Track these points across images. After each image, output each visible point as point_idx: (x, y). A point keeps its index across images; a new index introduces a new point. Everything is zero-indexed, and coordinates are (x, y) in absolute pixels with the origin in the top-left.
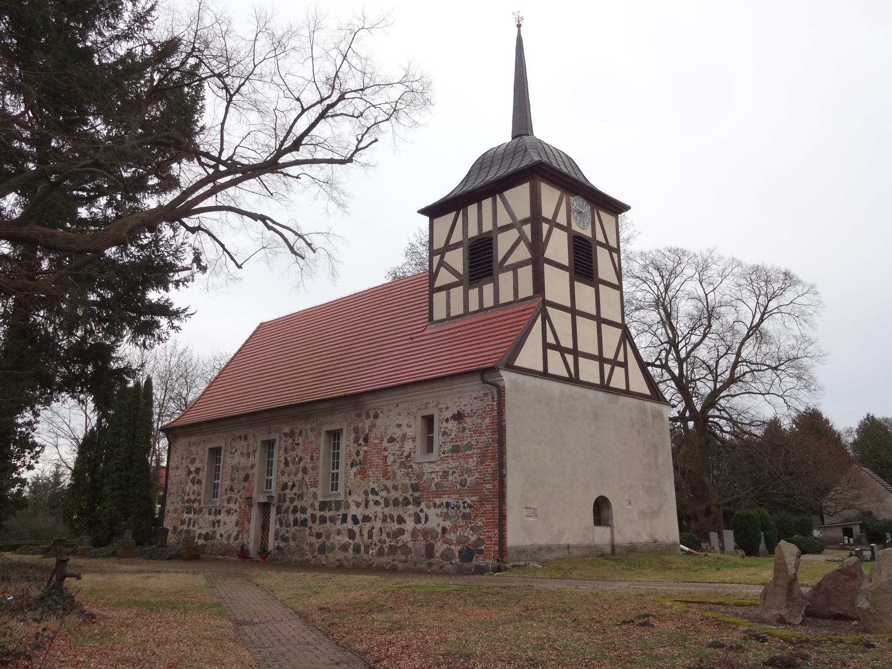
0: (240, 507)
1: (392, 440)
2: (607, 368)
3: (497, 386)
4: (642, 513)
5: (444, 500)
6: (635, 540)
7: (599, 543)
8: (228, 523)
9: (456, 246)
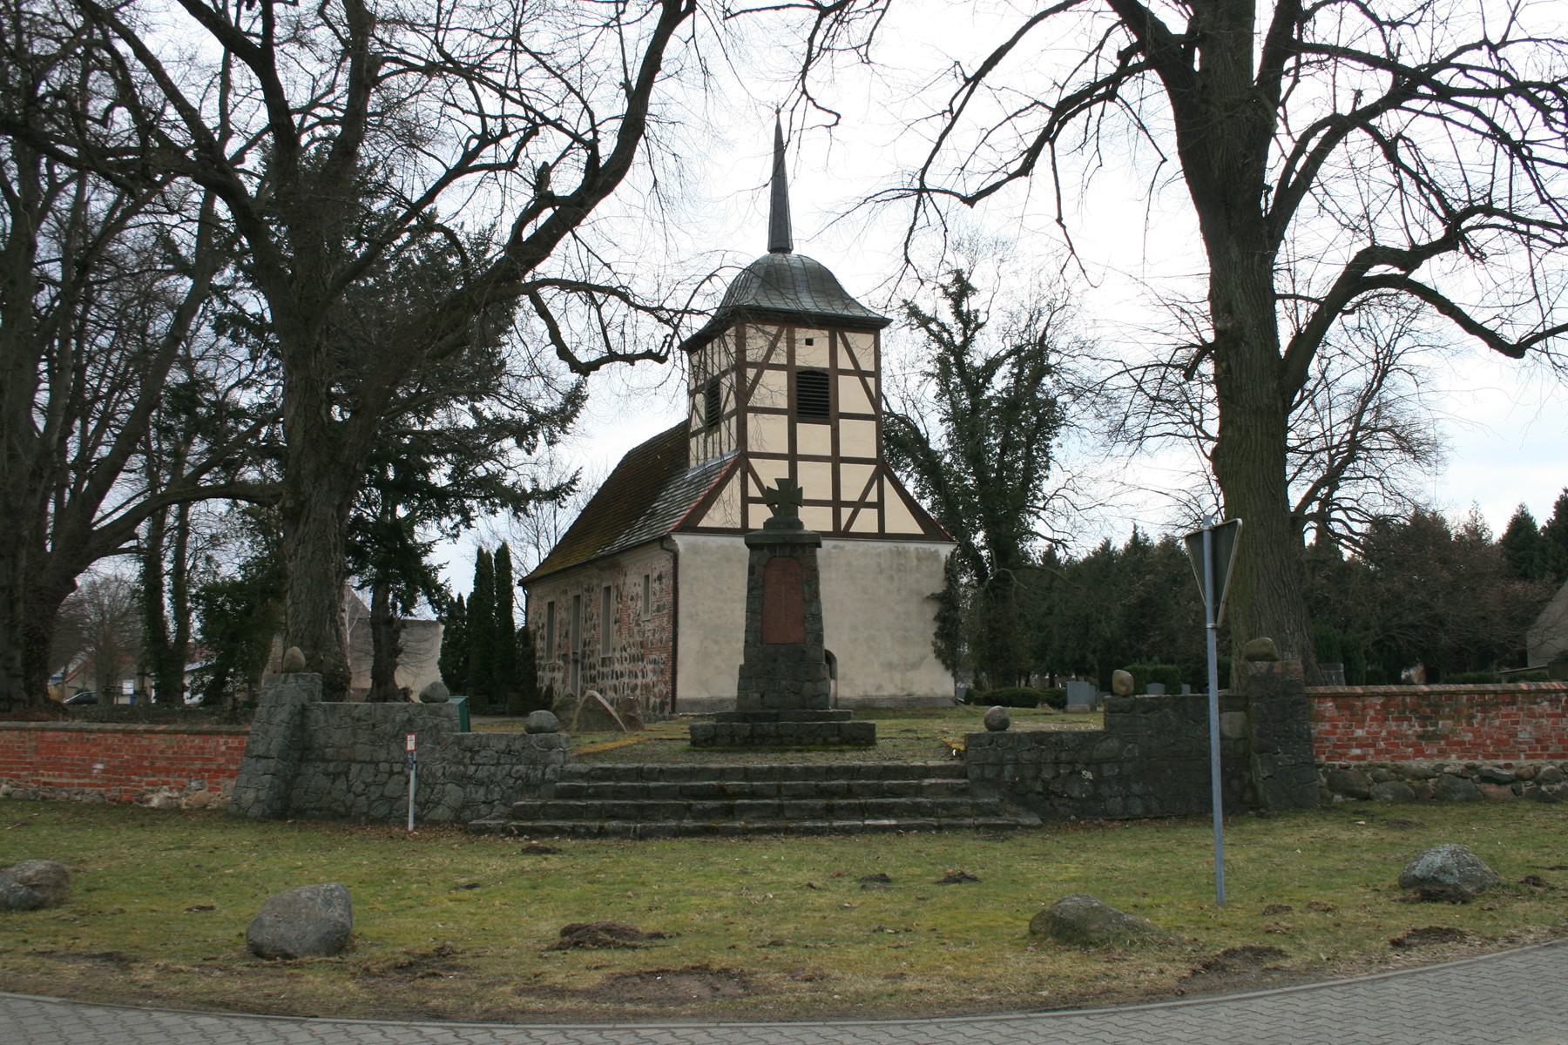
1: (632, 599)
2: (846, 513)
3: (671, 551)
4: (890, 666)
6: (873, 693)
9: (702, 385)
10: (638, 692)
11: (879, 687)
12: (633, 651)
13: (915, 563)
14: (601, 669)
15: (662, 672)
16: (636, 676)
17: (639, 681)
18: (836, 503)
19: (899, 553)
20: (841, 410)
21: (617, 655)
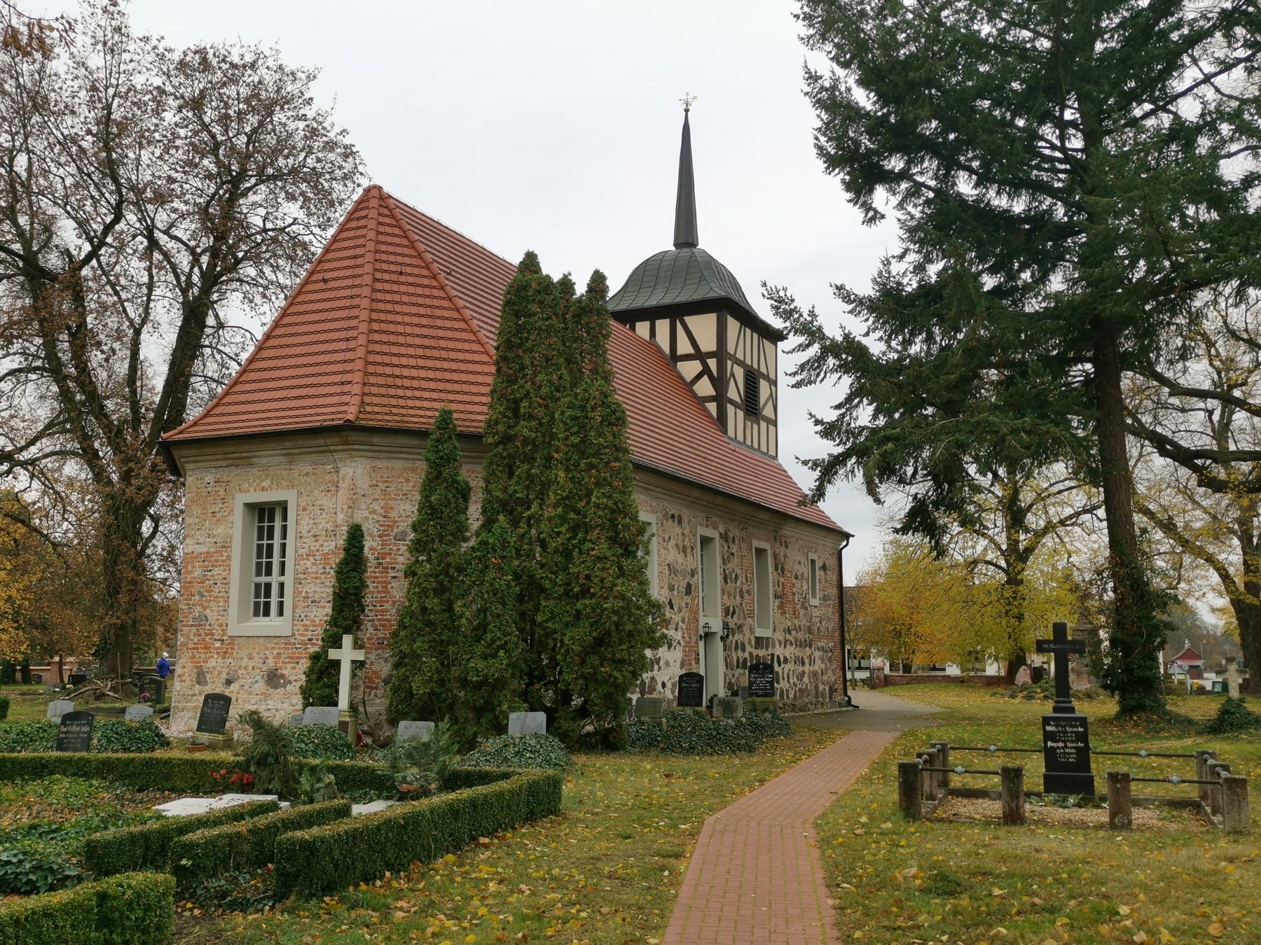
0: (683, 637)
5: (823, 644)
8: (672, 663)
10: (806, 679)
12: (801, 635)
14: (755, 652)
15: (830, 660)
16: (803, 664)
17: (807, 668)
21: (779, 636)
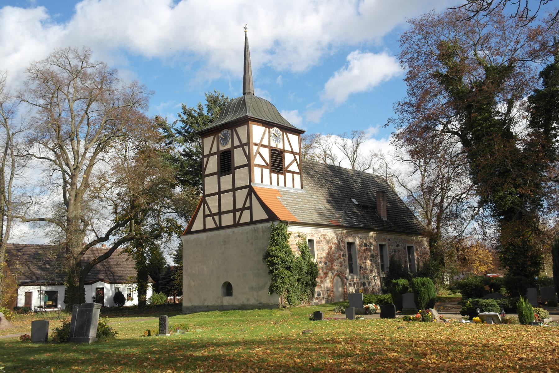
2: (238, 214)
4: (252, 288)
6: (246, 303)
7: (227, 304)
11: (248, 300)
13: (261, 234)
18: (234, 211)
19: (255, 230)
20: (236, 165)
